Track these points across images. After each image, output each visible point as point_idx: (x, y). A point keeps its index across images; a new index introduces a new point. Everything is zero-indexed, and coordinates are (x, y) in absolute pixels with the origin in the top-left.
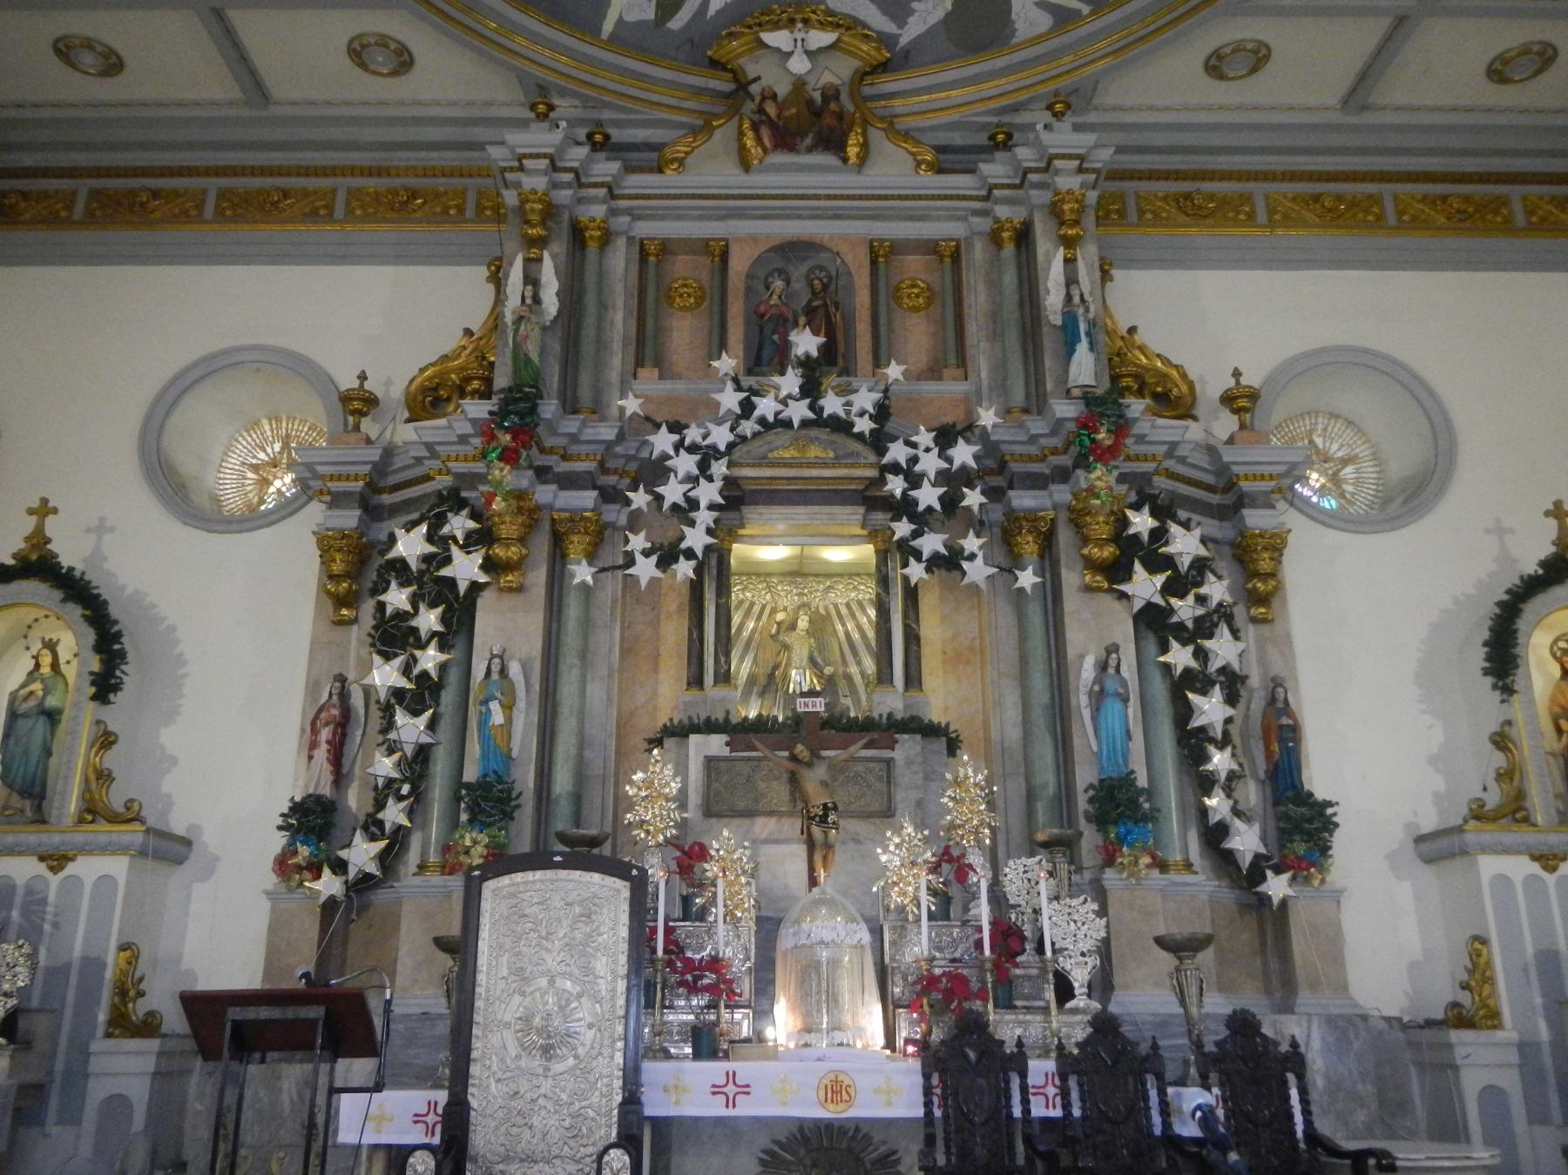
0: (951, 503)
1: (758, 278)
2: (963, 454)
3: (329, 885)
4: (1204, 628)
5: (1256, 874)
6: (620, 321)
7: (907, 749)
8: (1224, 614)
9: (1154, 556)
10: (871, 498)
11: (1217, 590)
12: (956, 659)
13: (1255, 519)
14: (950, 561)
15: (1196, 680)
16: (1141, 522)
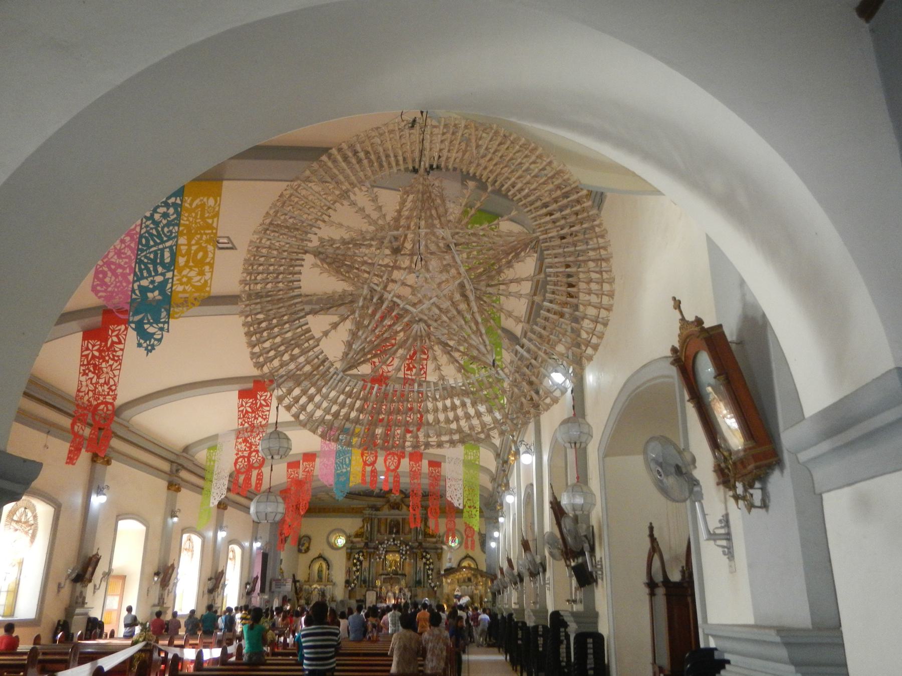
0: (406, 553)
1: (391, 521)
2: (408, 547)
3: (350, 588)
4: (430, 564)
5: (434, 587)
6: (376, 528)
7: (400, 577)
8: (432, 563)
9: (425, 557)
10: (398, 552)
11: (431, 561)
12: (410, 564)
13: (439, 551)
14: (406, 559)
15: (429, 569)
16: (424, 554)
